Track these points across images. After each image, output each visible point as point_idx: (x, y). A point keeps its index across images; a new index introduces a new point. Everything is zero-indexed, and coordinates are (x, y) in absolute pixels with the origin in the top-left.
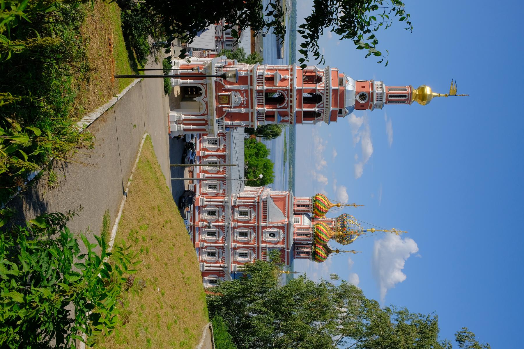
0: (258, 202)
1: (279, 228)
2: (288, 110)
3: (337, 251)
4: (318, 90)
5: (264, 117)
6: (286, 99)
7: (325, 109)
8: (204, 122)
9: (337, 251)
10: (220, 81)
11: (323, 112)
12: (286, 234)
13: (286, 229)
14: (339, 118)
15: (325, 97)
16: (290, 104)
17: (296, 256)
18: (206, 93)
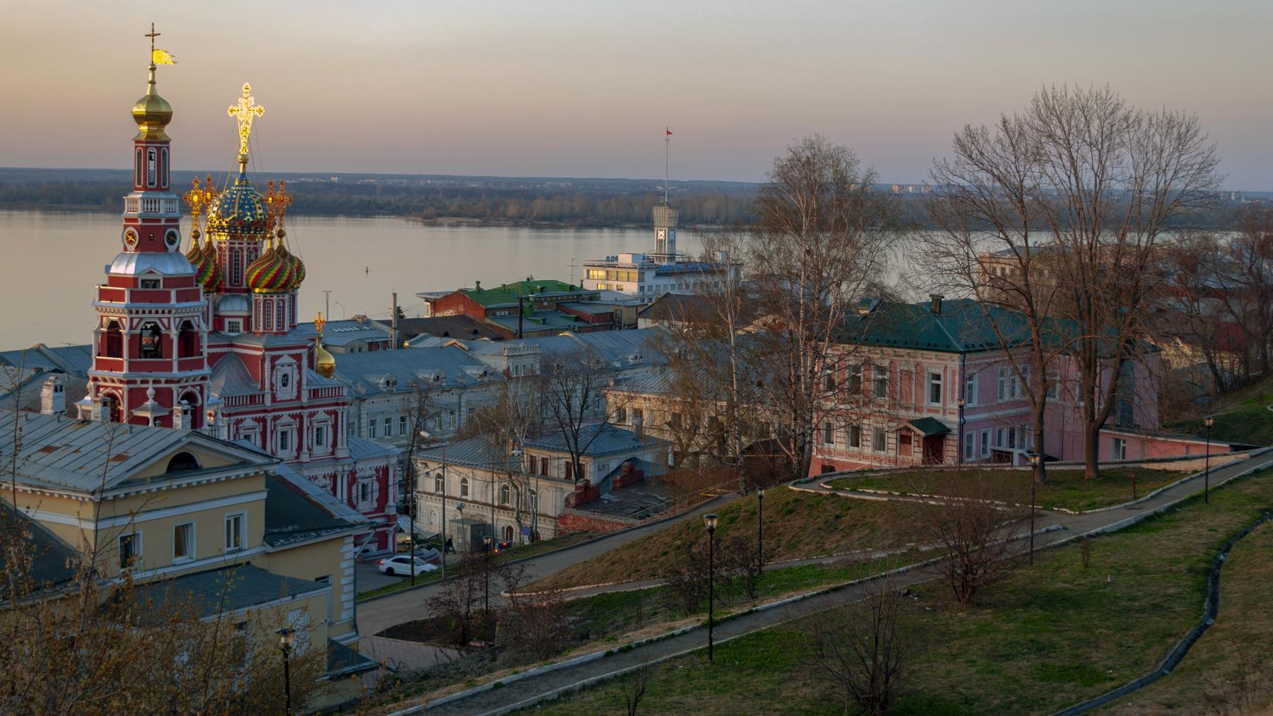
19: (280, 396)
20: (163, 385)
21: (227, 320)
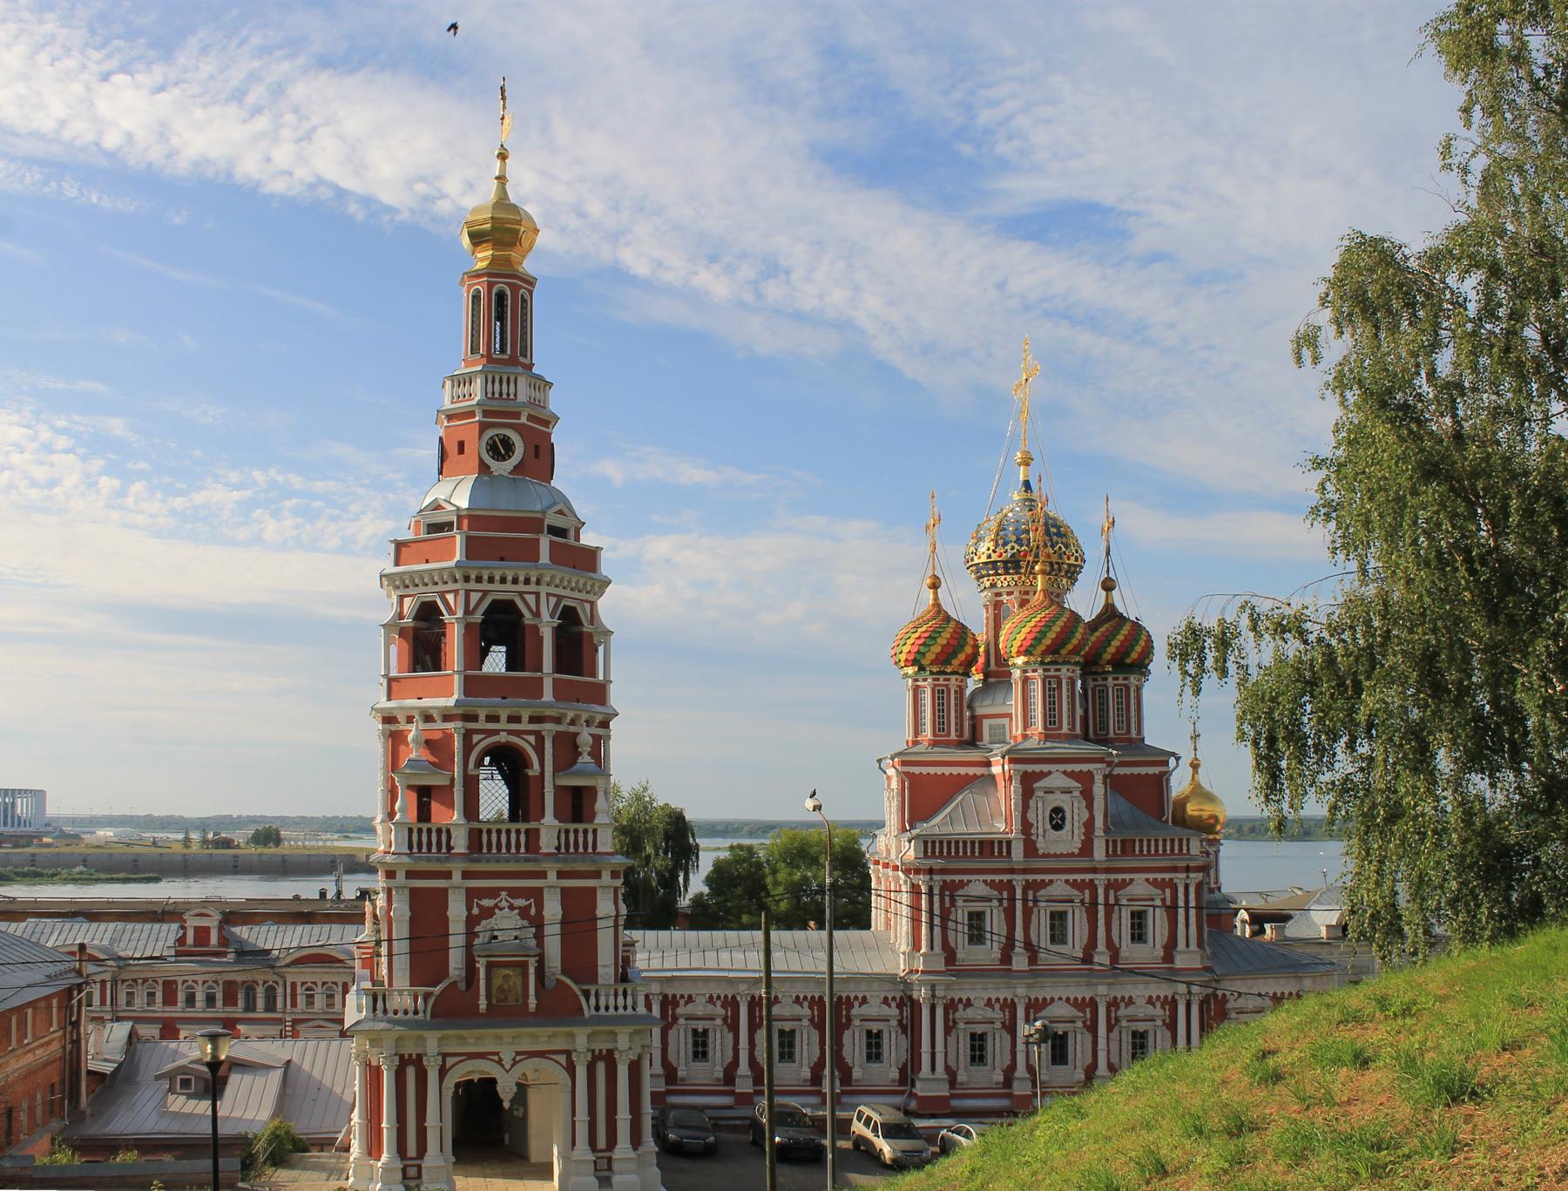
0: (931, 871)
1: (1027, 794)
2: (548, 729)
3: (1108, 585)
4: (467, 612)
5: (581, 827)
6: (503, 738)
7: (543, 590)
8: (601, 1067)
9: (1108, 585)
10: (431, 1001)
11: (560, 598)
13: (1030, 768)
14: (587, 539)
15: (497, 586)
16: (524, 726)
17: (1134, 734)
18: (482, 1056)
19: (1041, 845)
21: (986, 723)
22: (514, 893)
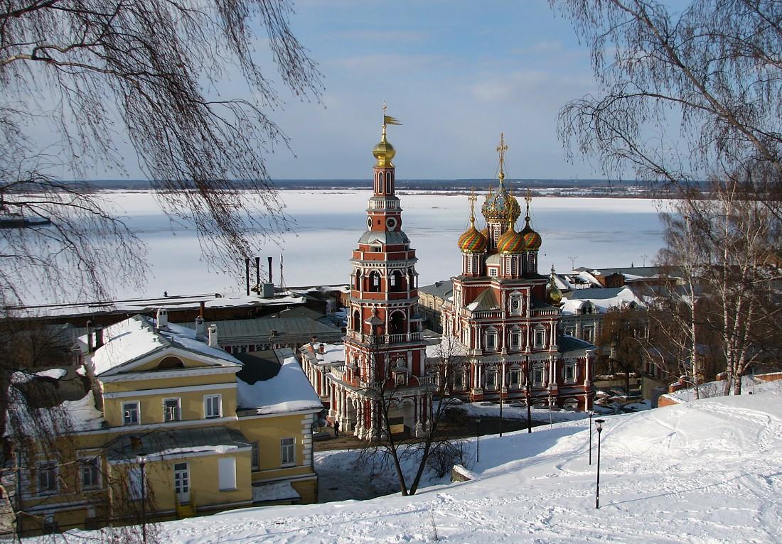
0: (478, 323)
3: (527, 219)
9: (527, 219)
12: (515, 288)
13: (508, 289)
16: (403, 306)
20: (380, 307)
21: (489, 268)
22: (400, 353)
